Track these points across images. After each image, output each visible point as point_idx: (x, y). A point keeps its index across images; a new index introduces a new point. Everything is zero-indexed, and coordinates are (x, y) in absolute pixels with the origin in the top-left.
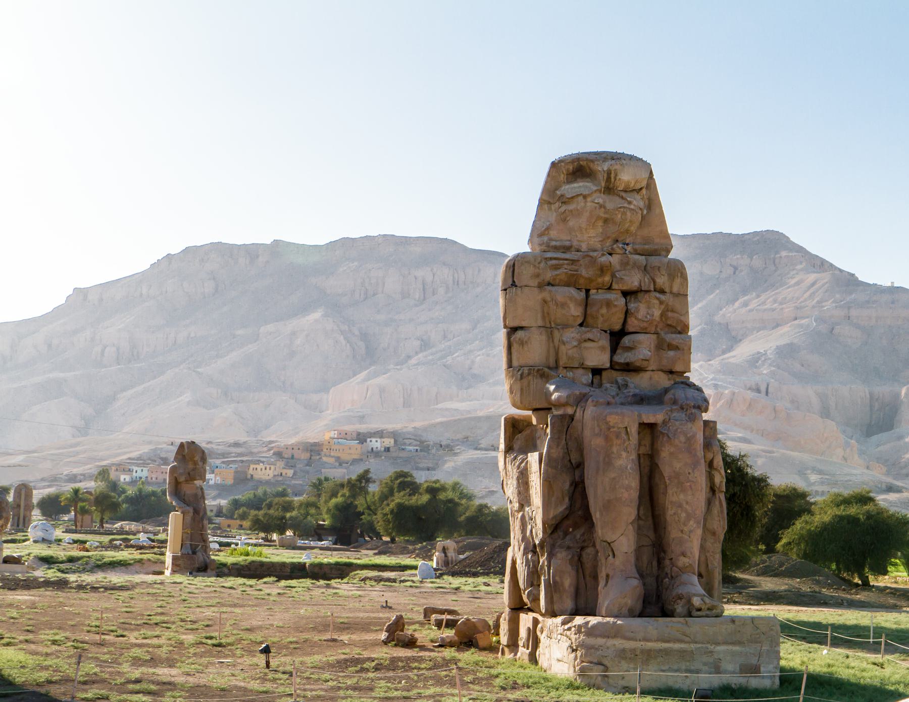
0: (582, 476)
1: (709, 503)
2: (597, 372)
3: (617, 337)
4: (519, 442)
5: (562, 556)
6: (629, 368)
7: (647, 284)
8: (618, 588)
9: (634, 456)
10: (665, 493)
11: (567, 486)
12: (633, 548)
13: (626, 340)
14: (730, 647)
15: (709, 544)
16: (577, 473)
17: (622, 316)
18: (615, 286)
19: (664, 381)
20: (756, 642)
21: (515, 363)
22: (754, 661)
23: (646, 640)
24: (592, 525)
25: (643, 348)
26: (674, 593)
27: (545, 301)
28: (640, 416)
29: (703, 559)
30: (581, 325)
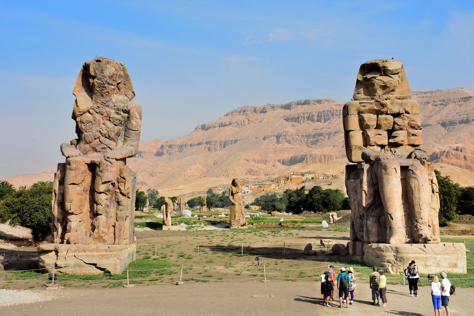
2: (382, 147)
4: (353, 176)
6: (396, 145)
7: (402, 111)
10: (413, 193)
13: (394, 134)
14: (444, 256)
15: (432, 214)
17: (392, 124)
20: (455, 254)
22: (455, 261)
23: (407, 253)
25: (401, 136)
28: (400, 163)
29: (430, 220)
30: (375, 128)
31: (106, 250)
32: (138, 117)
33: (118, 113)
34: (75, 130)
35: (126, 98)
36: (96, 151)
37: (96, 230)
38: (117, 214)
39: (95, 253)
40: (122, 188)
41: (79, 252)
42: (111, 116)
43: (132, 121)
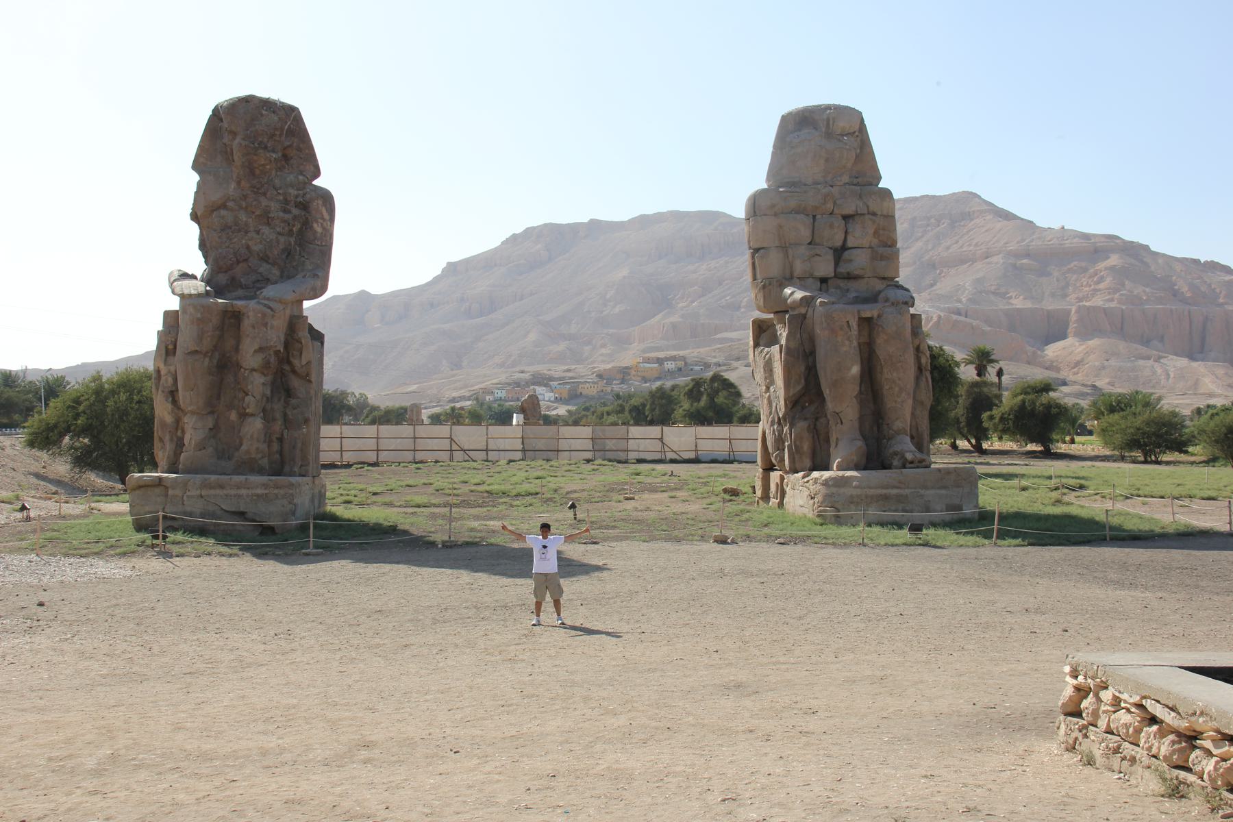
0: (814, 362)
1: (917, 379)
2: (824, 280)
3: (839, 253)
5: (802, 425)
8: (844, 448)
9: (855, 343)
11: (803, 368)
12: (857, 416)
13: (846, 254)
16: (810, 359)
18: (836, 211)
19: (879, 285)
21: (758, 276)
24: (824, 400)
26: (891, 451)
27: (780, 226)
28: (859, 312)
30: (810, 244)
31: (265, 486)
32: (326, 216)
33: (285, 211)
34: (197, 243)
35: (301, 177)
36: (241, 287)
37: (244, 448)
38: (285, 415)
39: (243, 492)
40: (296, 362)
41: (211, 488)
42: (271, 215)
43: (315, 225)
